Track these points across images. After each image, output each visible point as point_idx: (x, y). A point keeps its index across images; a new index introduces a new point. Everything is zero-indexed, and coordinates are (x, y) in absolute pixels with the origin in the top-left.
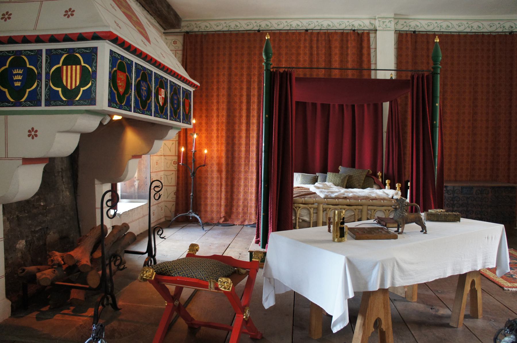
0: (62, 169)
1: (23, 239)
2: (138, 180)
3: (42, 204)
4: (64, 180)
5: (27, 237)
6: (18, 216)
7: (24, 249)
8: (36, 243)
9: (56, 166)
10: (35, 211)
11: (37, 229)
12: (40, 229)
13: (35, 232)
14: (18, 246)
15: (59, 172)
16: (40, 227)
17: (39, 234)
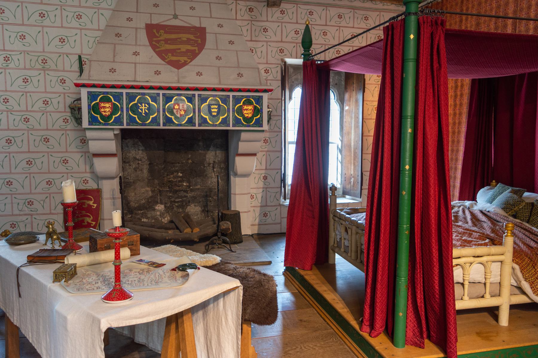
0: (214, 162)
1: (161, 203)
2: (353, 177)
3: (185, 184)
4: (215, 170)
5: (166, 203)
6: (159, 189)
7: (162, 211)
8: (175, 209)
9: (207, 160)
10: (177, 188)
11: (177, 200)
12: (180, 201)
13: (175, 202)
14: (157, 208)
15: (209, 164)
16: (181, 200)
17: (179, 204)
